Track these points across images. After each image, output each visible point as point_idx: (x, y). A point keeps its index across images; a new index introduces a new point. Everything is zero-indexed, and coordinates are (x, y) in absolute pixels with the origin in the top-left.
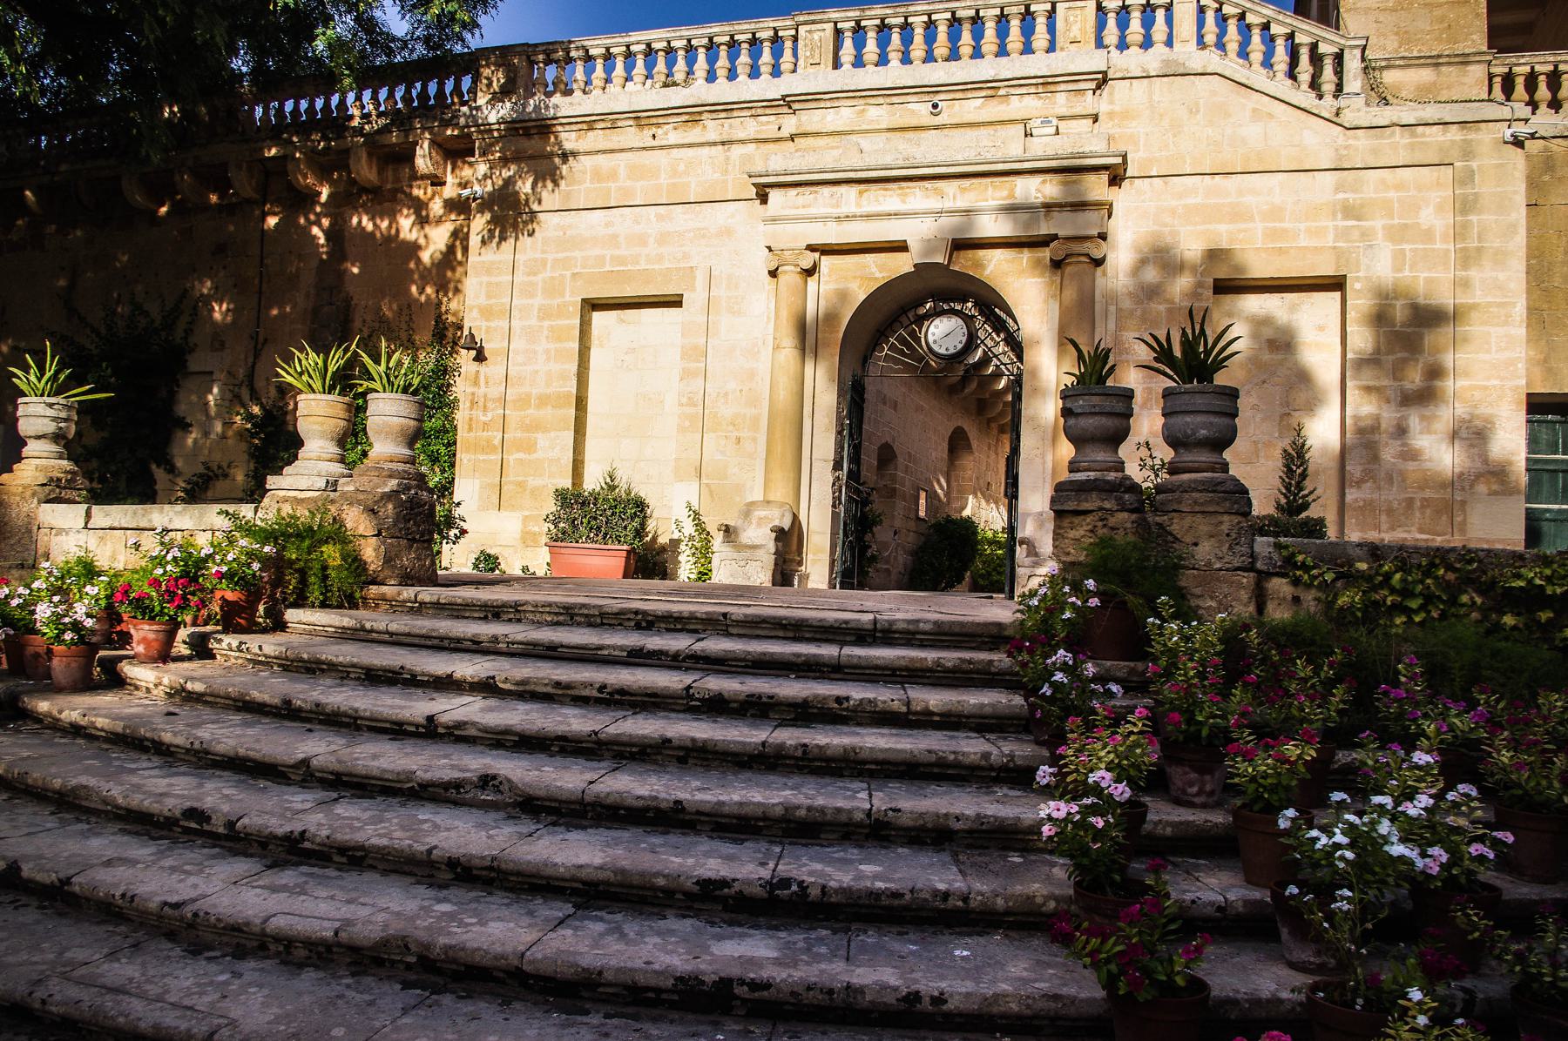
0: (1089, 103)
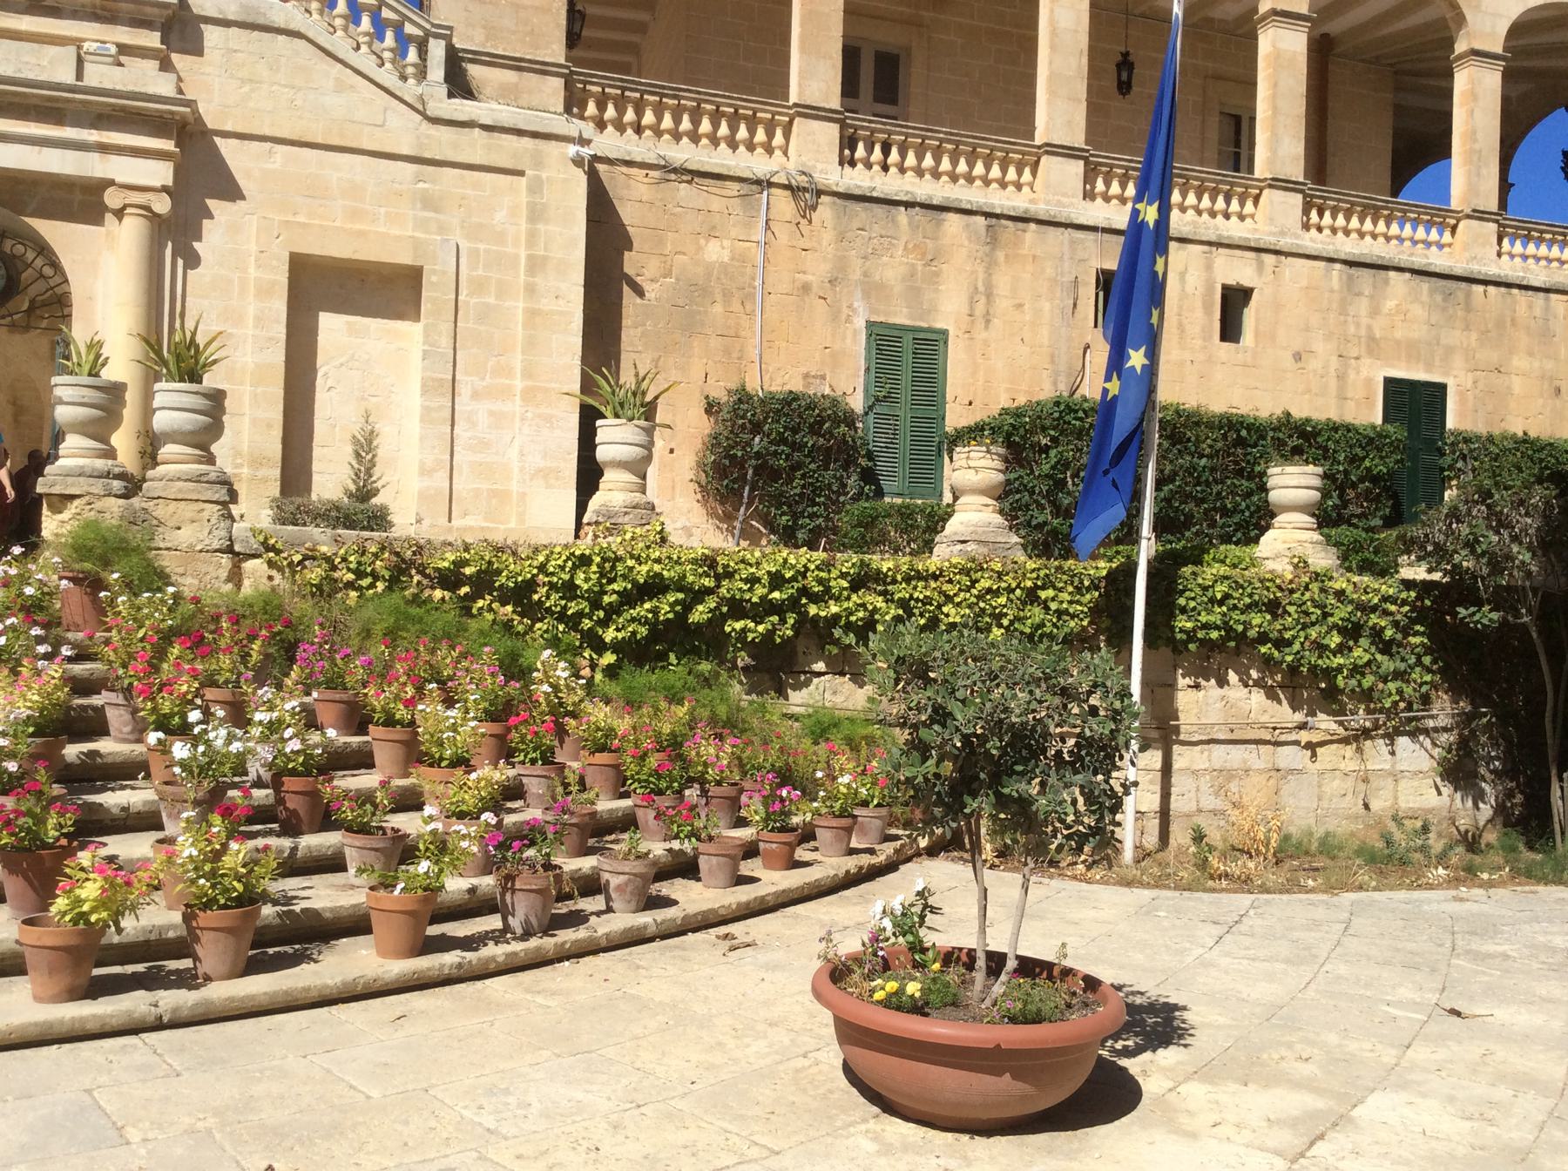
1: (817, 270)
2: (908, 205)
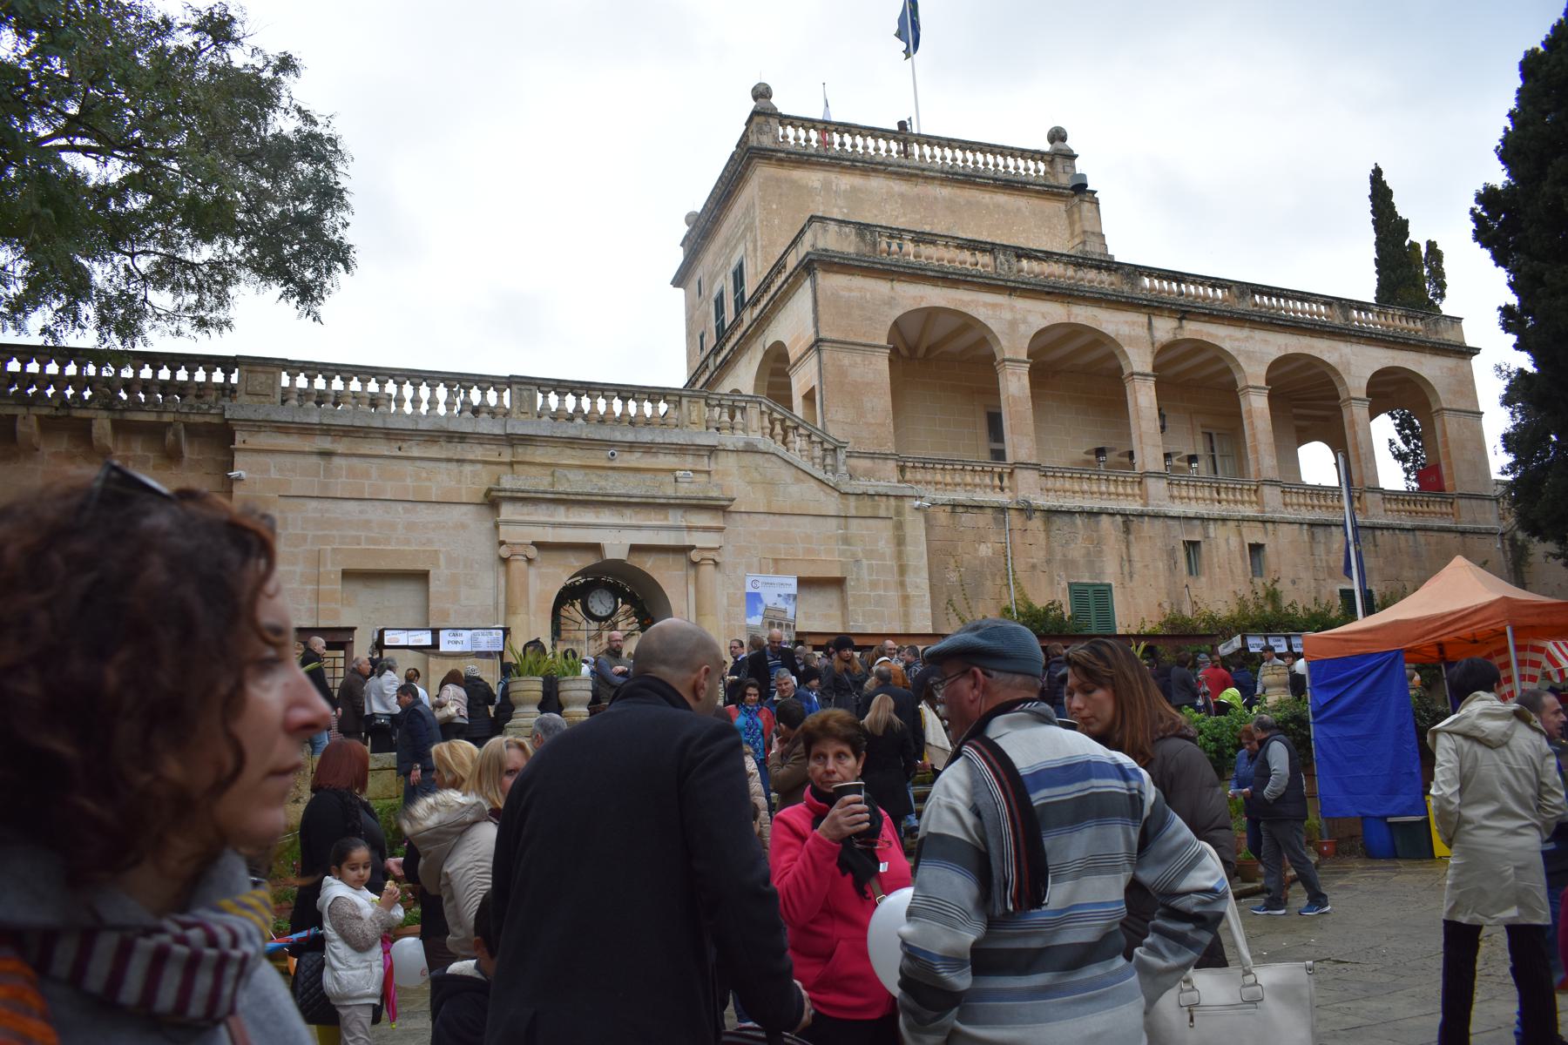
0: (704, 464)
1: (1039, 556)
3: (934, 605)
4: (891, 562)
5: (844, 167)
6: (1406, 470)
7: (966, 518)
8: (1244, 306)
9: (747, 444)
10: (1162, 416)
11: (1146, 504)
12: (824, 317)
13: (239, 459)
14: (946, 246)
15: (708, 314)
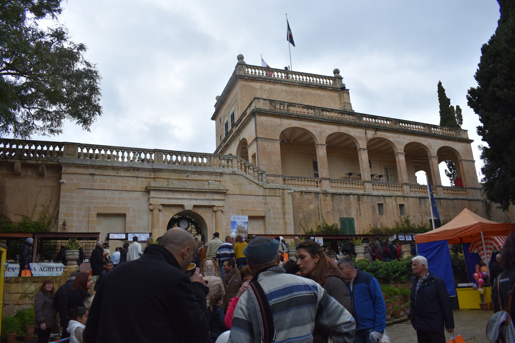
0: (218, 178)
1: (330, 209)
2: (344, 194)
3: (295, 225)
4: (280, 211)
5: (267, 82)
6: (451, 180)
7: (305, 196)
8: (396, 126)
9: (233, 172)
10: (370, 162)
11: (365, 191)
12: (259, 130)
13: (63, 176)
14: (299, 107)
15: (223, 129)
